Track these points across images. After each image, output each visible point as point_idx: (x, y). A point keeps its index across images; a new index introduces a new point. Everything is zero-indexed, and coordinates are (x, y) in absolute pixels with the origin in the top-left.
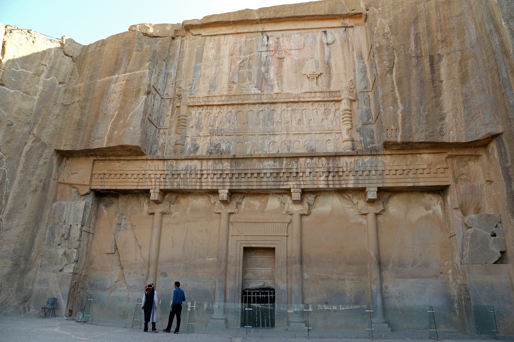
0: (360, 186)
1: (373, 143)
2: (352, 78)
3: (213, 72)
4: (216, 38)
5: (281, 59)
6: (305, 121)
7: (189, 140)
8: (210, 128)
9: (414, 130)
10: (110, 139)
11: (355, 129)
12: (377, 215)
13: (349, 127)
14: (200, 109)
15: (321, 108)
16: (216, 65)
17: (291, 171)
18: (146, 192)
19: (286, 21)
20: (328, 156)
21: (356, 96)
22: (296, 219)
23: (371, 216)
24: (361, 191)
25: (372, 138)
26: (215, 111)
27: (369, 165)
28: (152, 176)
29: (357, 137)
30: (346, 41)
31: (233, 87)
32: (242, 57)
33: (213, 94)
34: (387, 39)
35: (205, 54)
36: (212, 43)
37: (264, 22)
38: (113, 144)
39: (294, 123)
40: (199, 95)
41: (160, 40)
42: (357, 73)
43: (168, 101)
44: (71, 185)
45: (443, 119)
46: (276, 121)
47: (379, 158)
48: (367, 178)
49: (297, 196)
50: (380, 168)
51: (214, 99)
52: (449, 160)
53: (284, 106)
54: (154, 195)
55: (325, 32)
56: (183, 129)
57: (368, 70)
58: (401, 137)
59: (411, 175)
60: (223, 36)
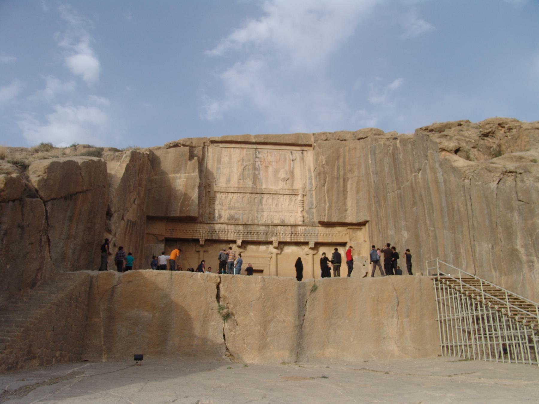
0: (307, 241)
1: (313, 219)
4: (228, 149)
5: (267, 167)
6: (280, 205)
7: (217, 212)
9: (333, 216)
10: (181, 211)
12: (313, 255)
13: (302, 209)
14: (222, 194)
15: (288, 198)
18: (197, 241)
20: (292, 226)
22: (274, 256)
23: (310, 256)
24: (306, 243)
25: (313, 216)
26: (230, 195)
29: (306, 215)
30: (302, 159)
32: (245, 164)
33: (229, 186)
34: (324, 168)
35: (222, 160)
38: (183, 215)
39: (274, 206)
40: (220, 185)
43: (203, 188)
44: (154, 235)
45: (346, 211)
47: (316, 228)
49: (275, 244)
52: (348, 230)
53: (269, 195)
54: (202, 242)
55: (291, 152)
59: (330, 236)
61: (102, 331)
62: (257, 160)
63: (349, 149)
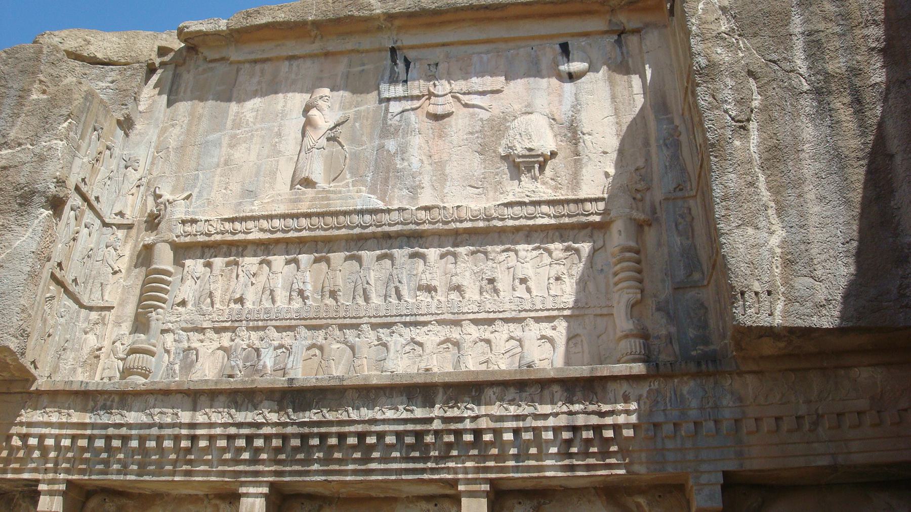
1: (706, 341)
2: (641, 163)
3: (253, 157)
4: (268, 67)
6: (504, 282)
8: (232, 305)
11: (651, 303)
16: (263, 137)
17: (460, 426)
19: (456, 21)
21: (654, 211)
25: (704, 325)
27: (694, 403)
28: (50, 442)
29: (659, 326)
31: (304, 193)
36: (255, 80)
37: (397, 23)
41: (113, 73)
42: (653, 149)
46: (424, 282)
48: (689, 444)
50: (727, 414)
51: (250, 224)
56: (156, 308)
57: (683, 138)
58: (786, 313)
60: (287, 63)
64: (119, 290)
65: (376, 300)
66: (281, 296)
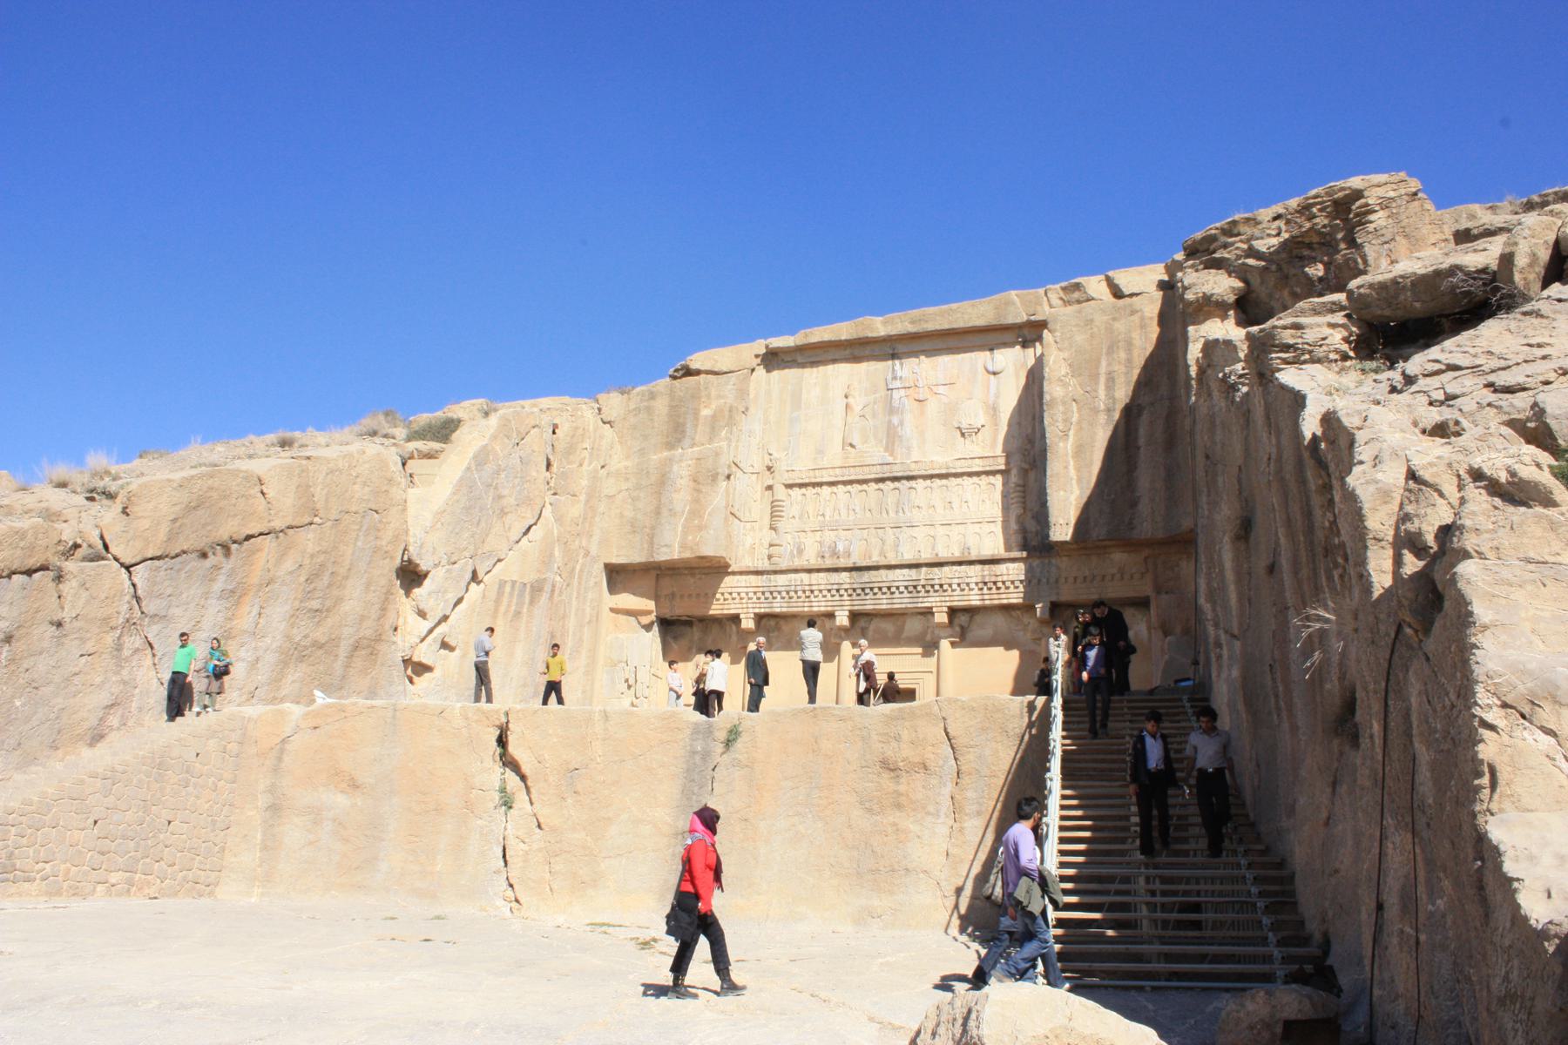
10: (683, 546)
11: (1029, 514)
18: (736, 619)
34: (1065, 385)
38: (687, 555)
45: (1134, 504)
54: (748, 623)
61: (259, 836)
62: (897, 384)
63: (1142, 318)
64: (758, 508)
65: (892, 514)
66: (844, 512)
